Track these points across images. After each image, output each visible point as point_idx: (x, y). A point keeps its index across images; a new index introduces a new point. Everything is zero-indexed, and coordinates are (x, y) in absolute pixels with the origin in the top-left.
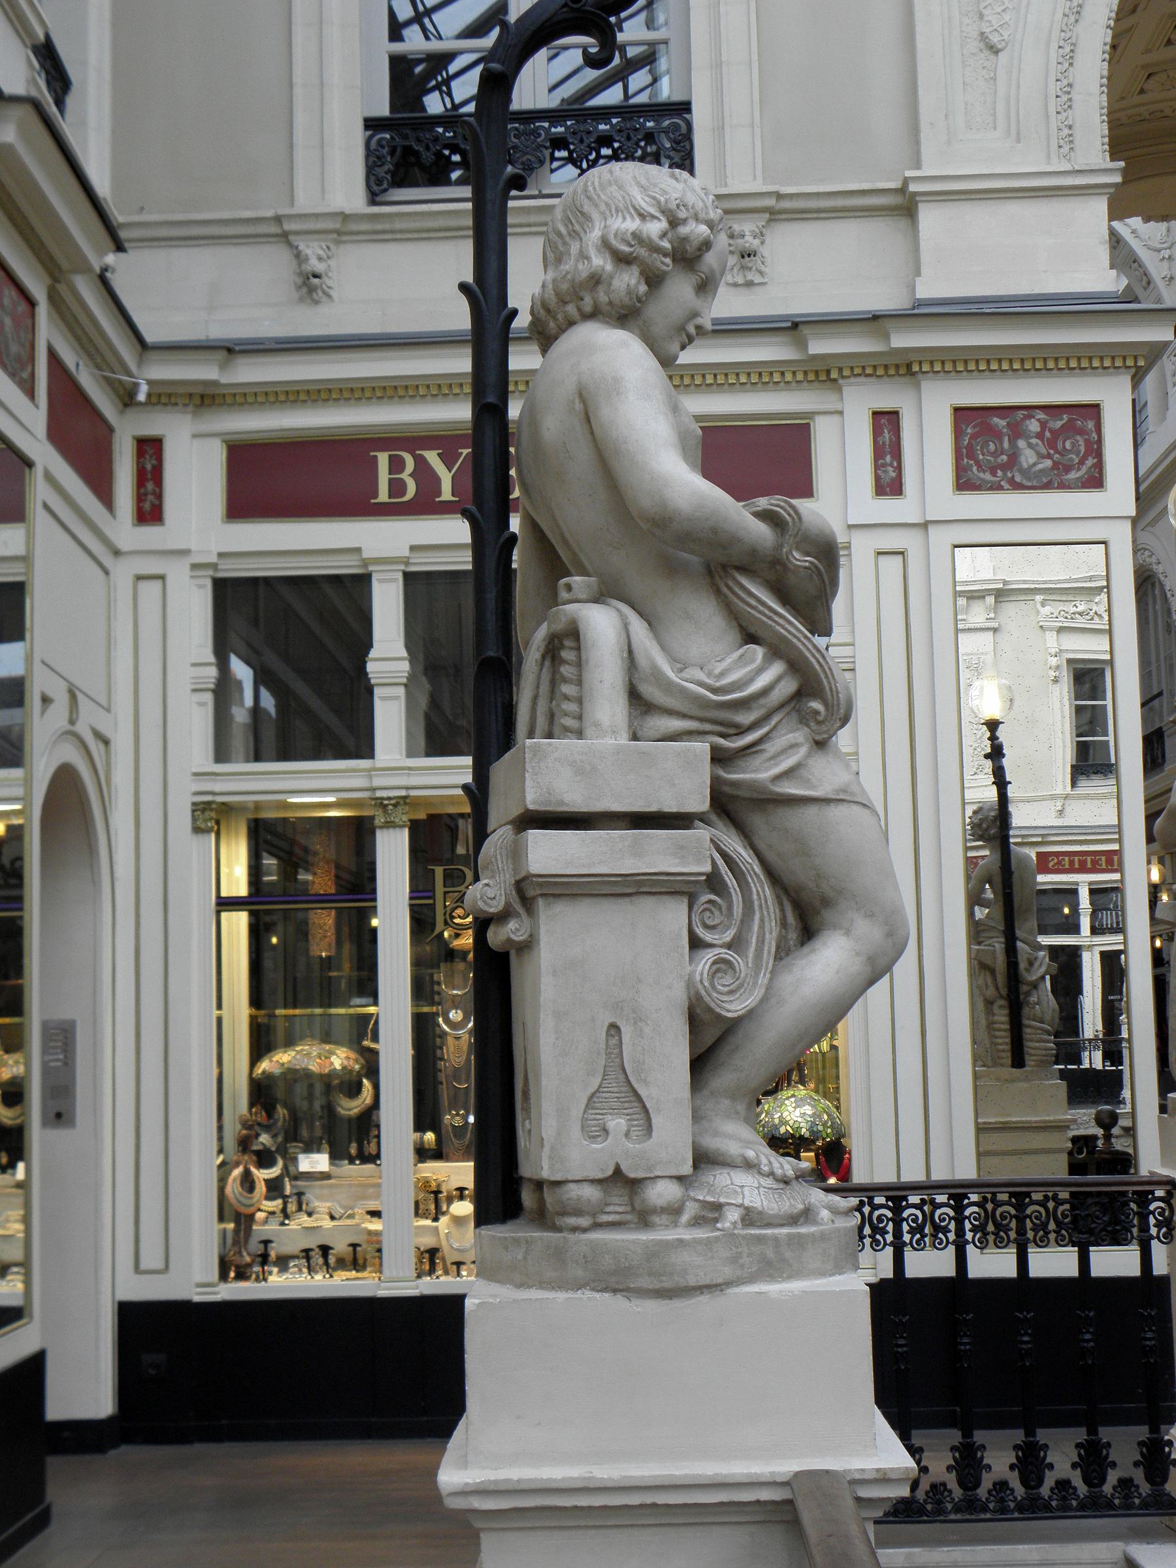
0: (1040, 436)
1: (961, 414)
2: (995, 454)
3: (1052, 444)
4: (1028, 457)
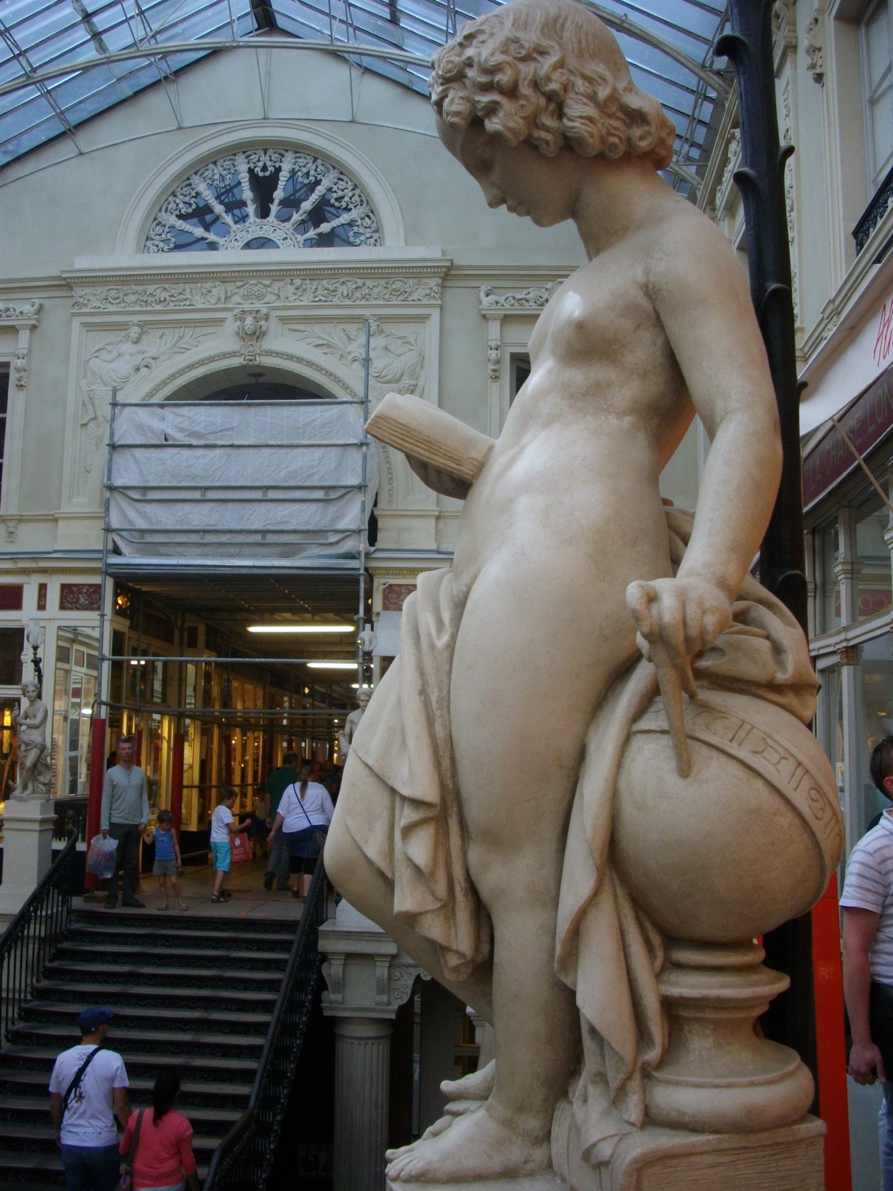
0: (86, 593)
1: (64, 587)
2: (72, 599)
3: (89, 596)
4: (82, 600)
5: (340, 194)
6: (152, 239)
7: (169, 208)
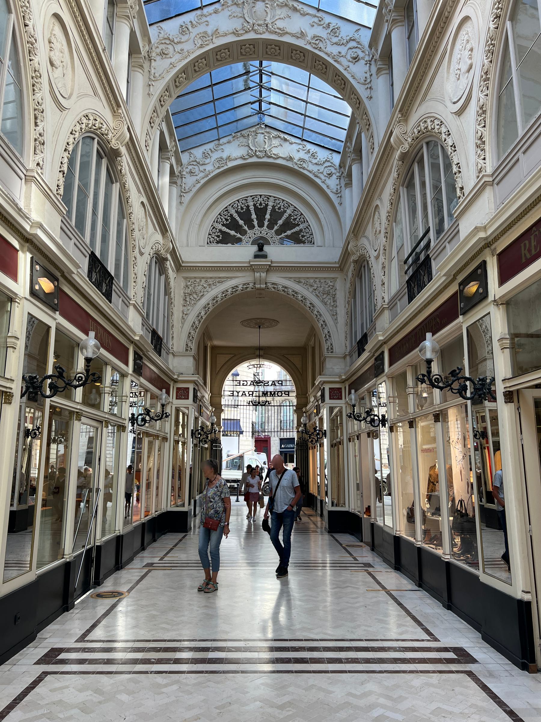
5: (295, 217)
6: (211, 235)
7: (218, 221)
